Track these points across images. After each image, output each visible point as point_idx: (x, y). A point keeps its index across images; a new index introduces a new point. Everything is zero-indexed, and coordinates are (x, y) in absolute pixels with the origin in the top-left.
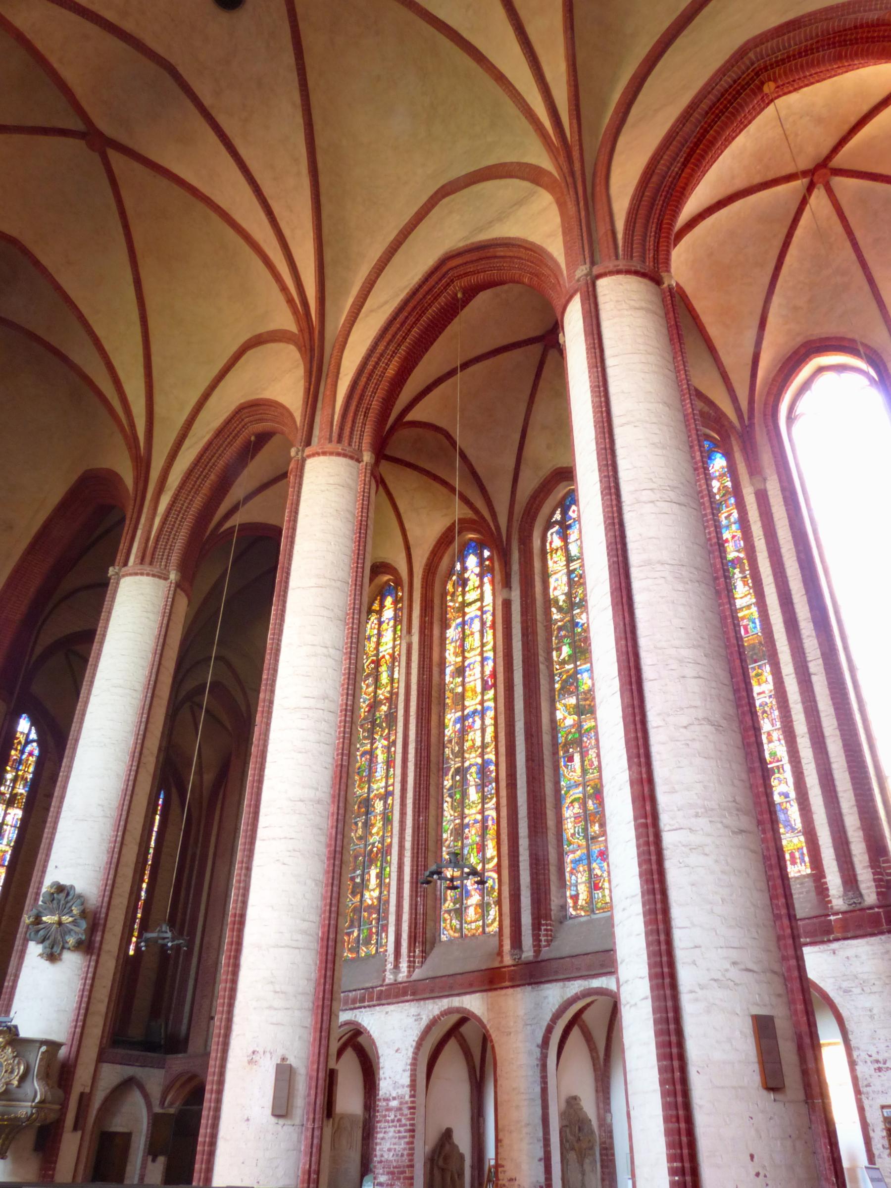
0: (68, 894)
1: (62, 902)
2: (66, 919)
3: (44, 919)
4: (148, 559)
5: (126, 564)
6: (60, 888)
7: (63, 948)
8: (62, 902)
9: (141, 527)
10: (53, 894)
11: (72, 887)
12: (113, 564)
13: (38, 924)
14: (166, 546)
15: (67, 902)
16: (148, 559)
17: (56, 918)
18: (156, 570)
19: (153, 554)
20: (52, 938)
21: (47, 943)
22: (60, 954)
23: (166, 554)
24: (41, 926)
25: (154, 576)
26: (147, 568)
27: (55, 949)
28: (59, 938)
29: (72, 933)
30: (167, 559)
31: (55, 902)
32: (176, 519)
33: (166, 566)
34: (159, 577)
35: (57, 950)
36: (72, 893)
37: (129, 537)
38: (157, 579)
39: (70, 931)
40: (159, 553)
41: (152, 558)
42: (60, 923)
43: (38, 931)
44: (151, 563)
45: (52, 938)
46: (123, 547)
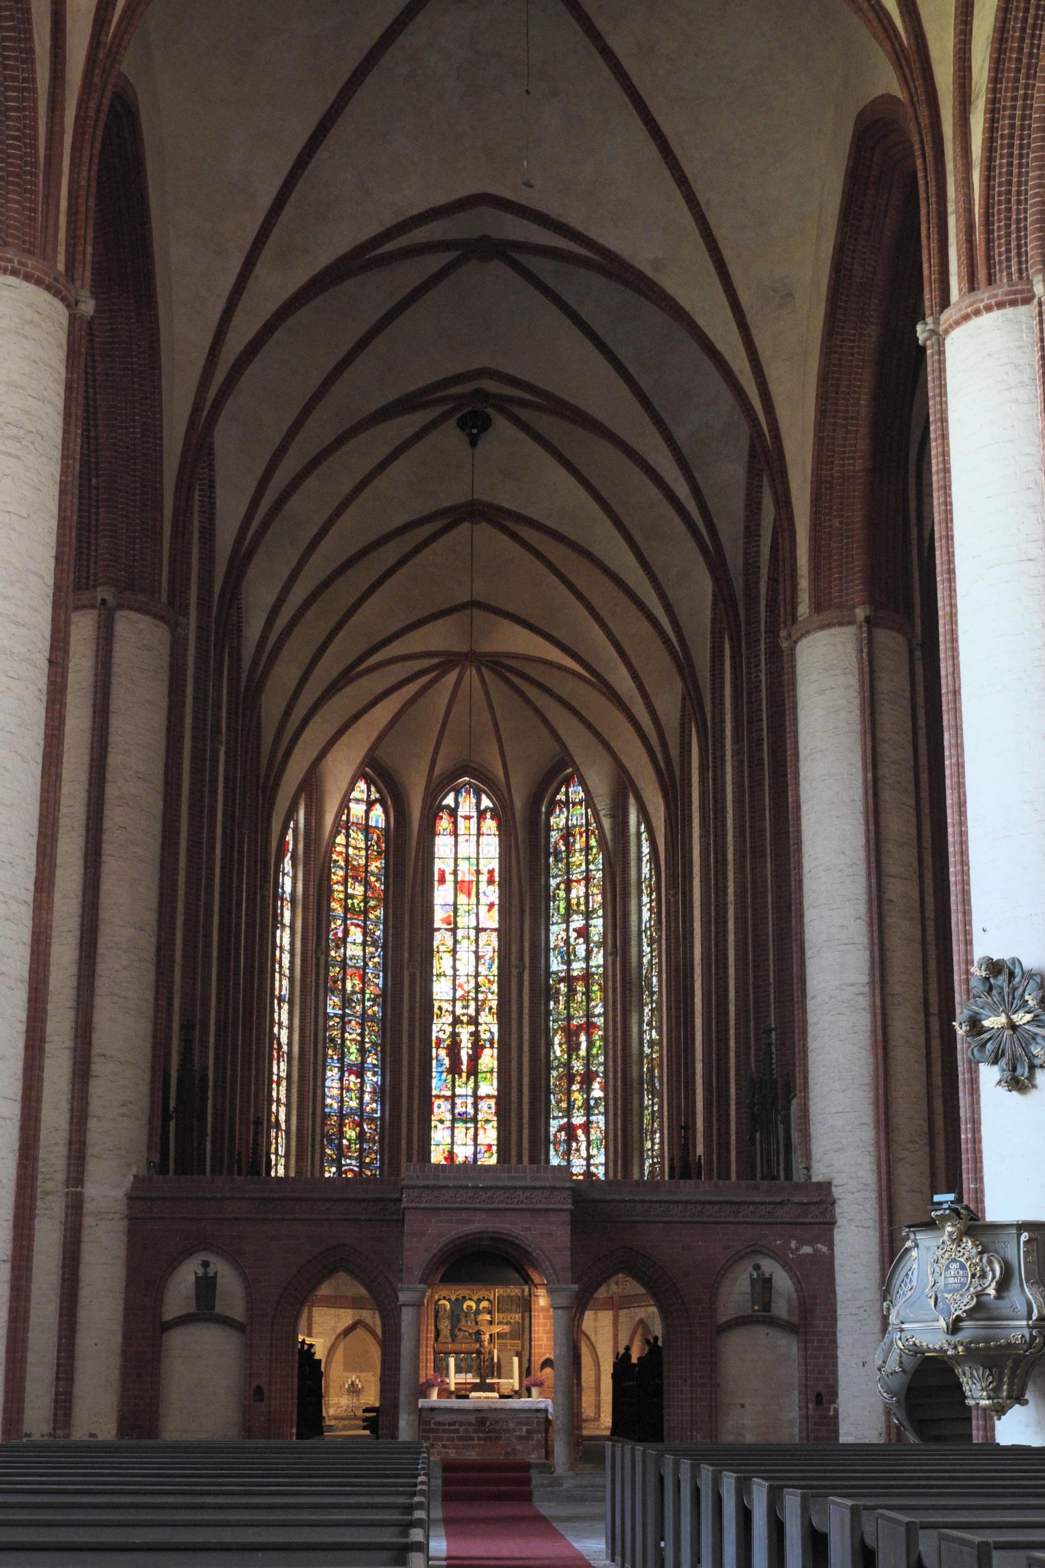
0: (1012, 975)
1: (1006, 990)
2: (1022, 1018)
3: (986, 1023)
4: (982, 274)
5: (945, 302)
6: (995, 967)
7: (1032, 1067)
8: (1006, 990)
9: (951, 207)
10: (987, 979)
11: (1016, 961)
12: (919, 316)
13: (980, 1033)
14: (1008, 226)
15: (1015, 989)
16: (982, 274)
17: (1002, 1020)
18: (1001, 291)
19: (989, 257)
20: (1008, 1053)
21: (1003, 1062)
22: (1031, 1077)
23: (1014, 244)
24: (986, 1036)
25: (1000, 305)
26: (984, 296)
27: (1019, 1071)
28: (1020, 1051)
29: (1039, 1040)
30: (1019, 255)
31: (994, 992)
32: (1011, 155)
33: (1020, 271)
34: (1013, 303)
35: (1023, 1071)
36: (1017, 971)
37: (934, 245)
38: (1009, 311)
39: (1034, 1037)
40: (999, 250)
41: (990, 267)
42: (1013, 1027)
43: (983, 1046)
44: (990, 281)
45: (1008, 1053)
46: (929, 270)
